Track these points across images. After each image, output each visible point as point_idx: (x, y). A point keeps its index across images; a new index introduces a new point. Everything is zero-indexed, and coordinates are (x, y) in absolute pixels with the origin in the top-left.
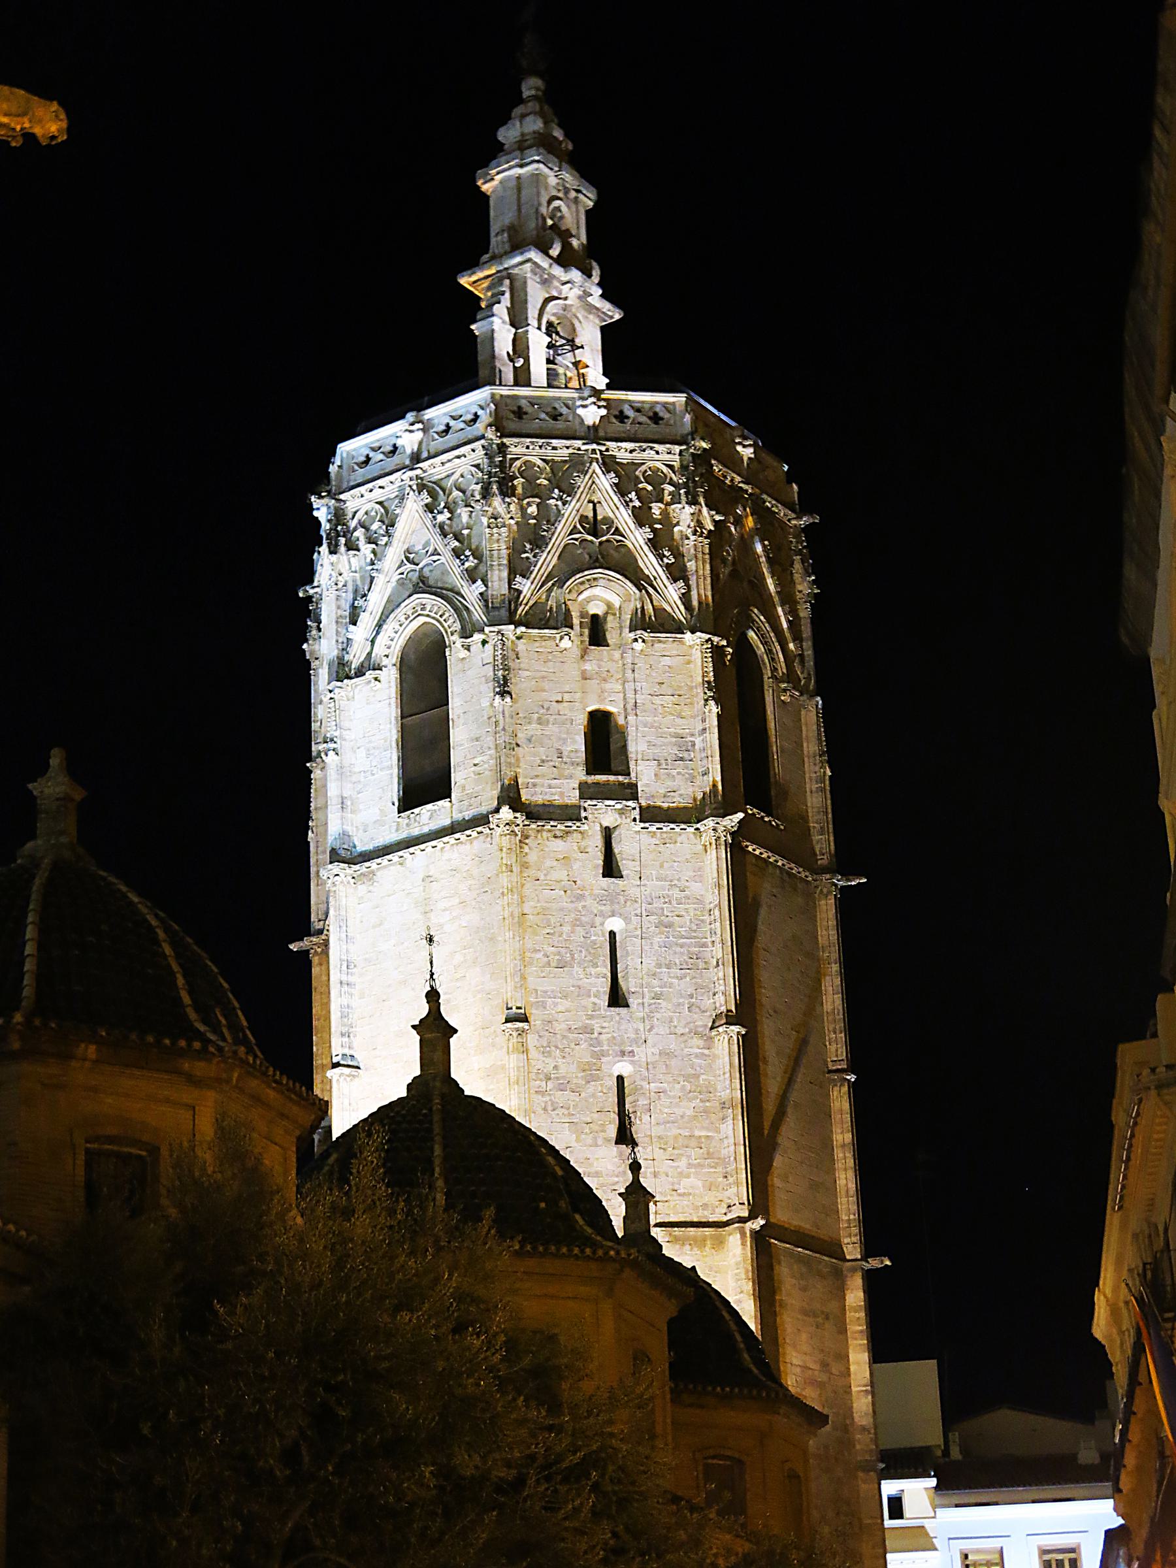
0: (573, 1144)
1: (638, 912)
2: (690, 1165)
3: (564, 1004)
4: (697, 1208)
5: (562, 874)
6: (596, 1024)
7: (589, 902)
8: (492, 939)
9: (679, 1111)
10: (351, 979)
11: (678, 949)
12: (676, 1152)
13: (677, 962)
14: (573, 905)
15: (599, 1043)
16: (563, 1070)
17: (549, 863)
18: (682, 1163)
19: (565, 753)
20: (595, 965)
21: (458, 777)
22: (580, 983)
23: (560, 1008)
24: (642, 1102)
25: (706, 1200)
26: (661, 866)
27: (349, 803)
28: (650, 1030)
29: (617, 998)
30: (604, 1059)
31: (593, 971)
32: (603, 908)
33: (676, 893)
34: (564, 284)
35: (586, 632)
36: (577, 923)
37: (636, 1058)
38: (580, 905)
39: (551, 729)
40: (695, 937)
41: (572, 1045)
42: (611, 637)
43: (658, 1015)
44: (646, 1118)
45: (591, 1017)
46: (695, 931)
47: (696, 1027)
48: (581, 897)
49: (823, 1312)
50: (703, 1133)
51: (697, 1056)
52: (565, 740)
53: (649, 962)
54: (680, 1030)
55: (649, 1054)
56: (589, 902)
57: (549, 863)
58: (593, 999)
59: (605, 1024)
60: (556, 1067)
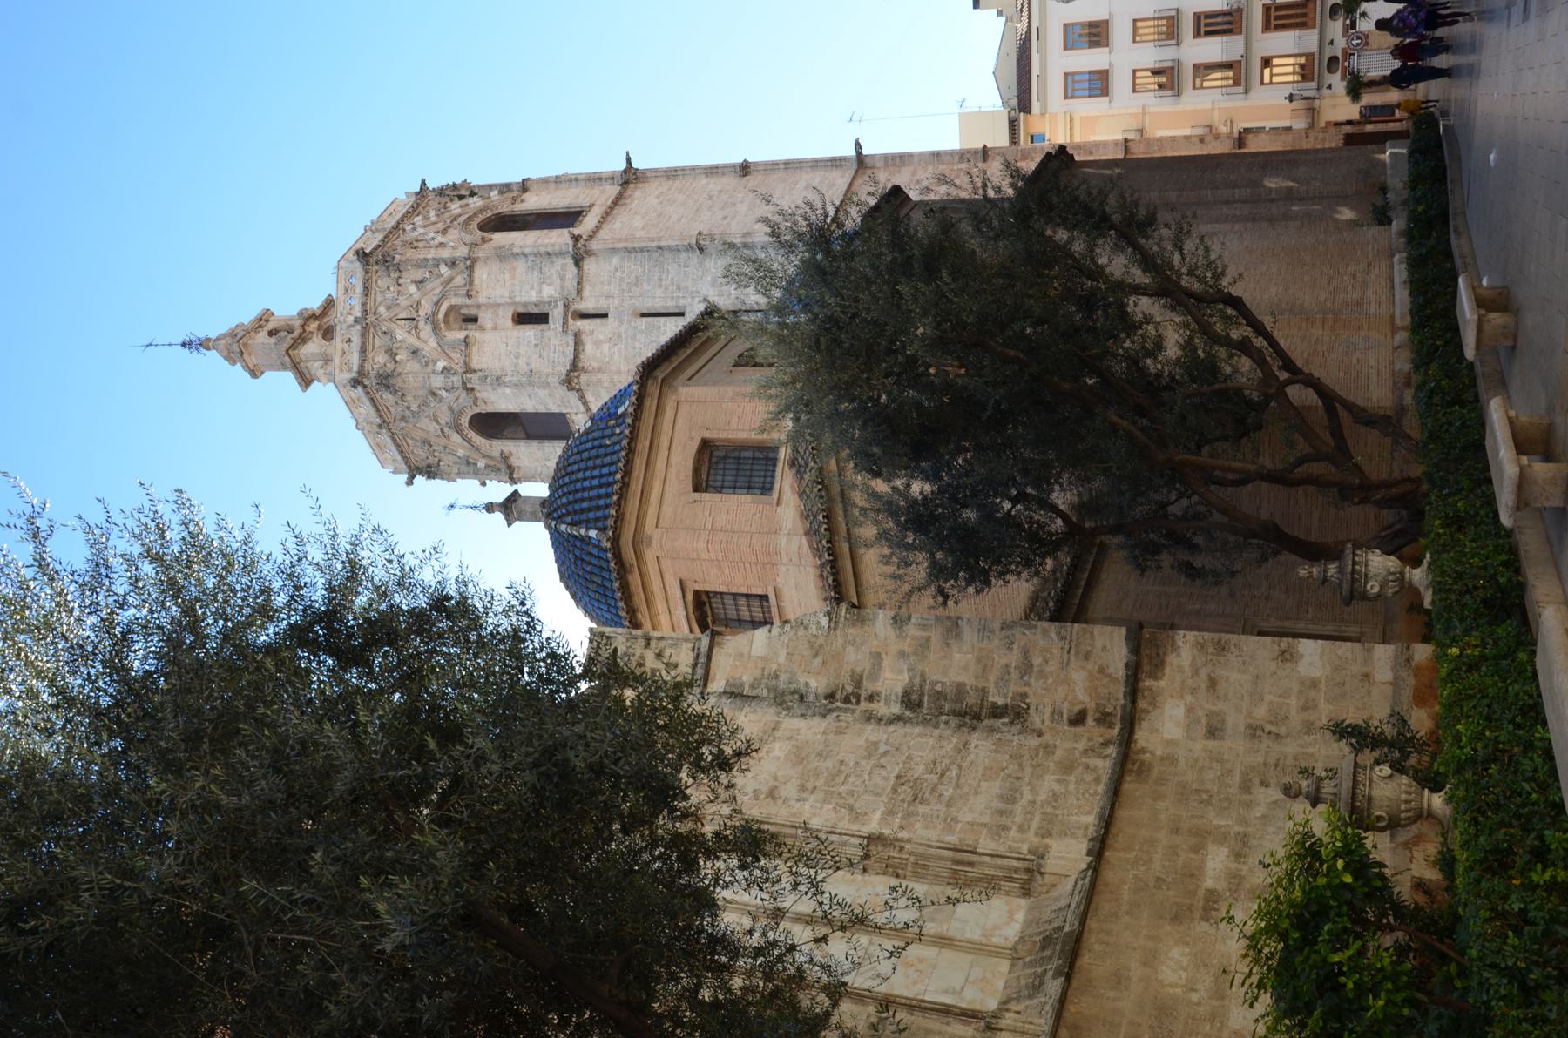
5: (606, 347)
36: (634, 338)
39: (522, 350)
42: (473, 312)
53: (659, 293)
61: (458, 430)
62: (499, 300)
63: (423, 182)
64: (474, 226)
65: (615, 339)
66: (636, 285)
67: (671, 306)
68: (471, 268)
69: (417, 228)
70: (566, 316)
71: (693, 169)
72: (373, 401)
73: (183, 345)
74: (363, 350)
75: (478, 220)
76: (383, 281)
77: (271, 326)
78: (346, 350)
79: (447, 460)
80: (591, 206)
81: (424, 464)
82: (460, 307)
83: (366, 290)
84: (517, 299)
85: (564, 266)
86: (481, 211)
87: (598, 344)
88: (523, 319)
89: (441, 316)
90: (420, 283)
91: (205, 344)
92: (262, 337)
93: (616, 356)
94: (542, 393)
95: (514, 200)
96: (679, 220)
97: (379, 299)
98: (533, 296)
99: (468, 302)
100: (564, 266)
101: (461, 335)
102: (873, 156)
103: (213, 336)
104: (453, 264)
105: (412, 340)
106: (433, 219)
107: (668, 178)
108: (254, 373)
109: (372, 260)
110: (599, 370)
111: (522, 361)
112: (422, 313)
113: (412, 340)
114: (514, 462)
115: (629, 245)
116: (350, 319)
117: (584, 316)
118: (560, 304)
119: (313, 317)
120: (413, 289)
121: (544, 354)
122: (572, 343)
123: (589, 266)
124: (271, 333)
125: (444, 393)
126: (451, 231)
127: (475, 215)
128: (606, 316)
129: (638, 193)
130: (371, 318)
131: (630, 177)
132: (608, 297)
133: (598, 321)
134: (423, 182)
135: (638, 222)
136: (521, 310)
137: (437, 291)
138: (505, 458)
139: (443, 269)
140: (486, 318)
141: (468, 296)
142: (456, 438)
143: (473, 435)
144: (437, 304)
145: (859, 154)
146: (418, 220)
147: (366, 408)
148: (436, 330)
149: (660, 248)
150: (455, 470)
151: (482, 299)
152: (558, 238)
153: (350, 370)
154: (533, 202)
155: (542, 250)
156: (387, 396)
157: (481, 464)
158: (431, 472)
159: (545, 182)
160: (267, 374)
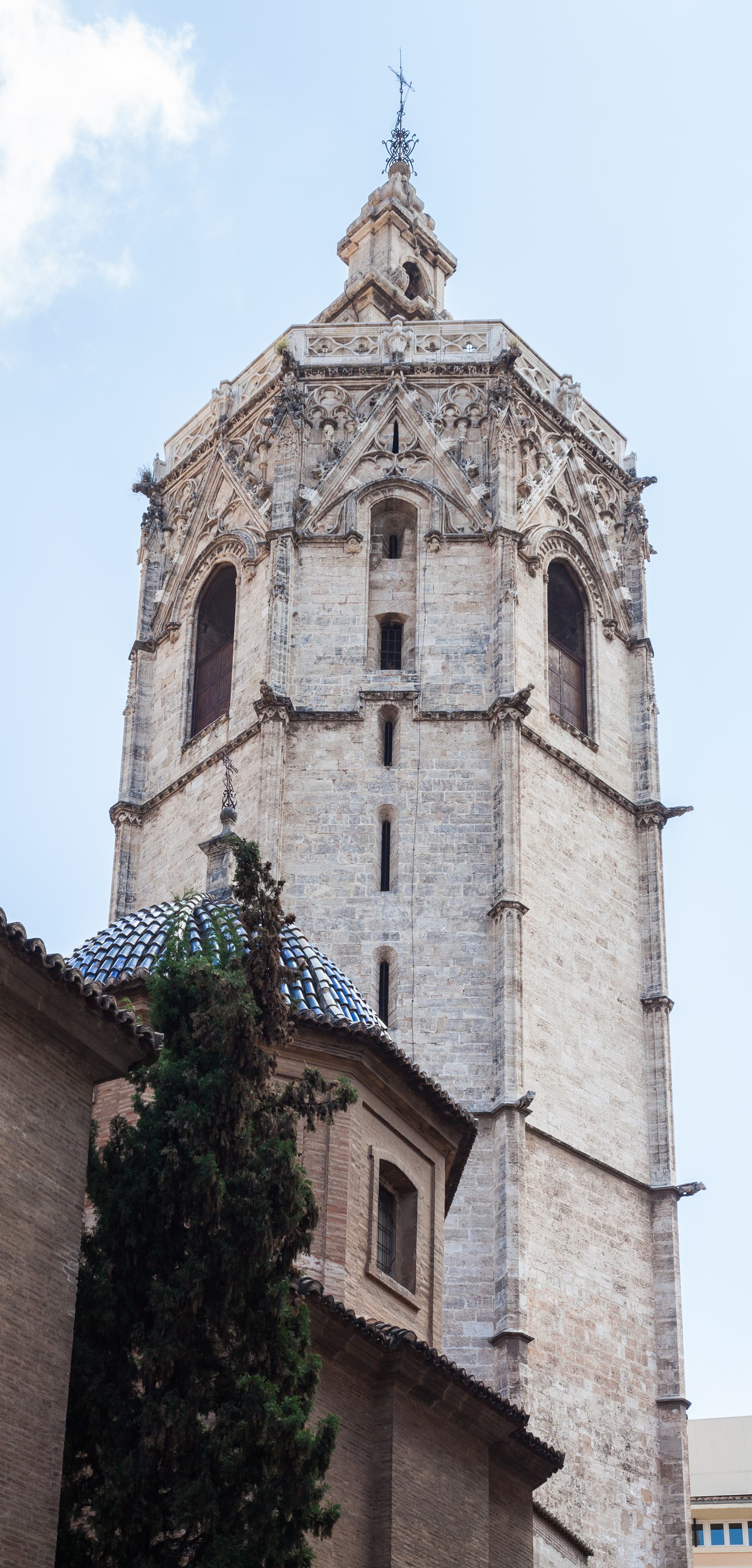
1: (415, 797)
2: (454, 1049)
3: (324, 889)
6: (358, 908)
7: (360, 789)
9: (446, 996)
11: (457, 834)
12: (439, 1035)
13: (455, 845)
14: (341, 793)
15: (360, 927)
19: (345, 650)
20: (361, 850)
22: (342, 868)
25: (471, 1085)
26: (444, 754)
27: (143, 752)
28: (418, 914)
29: (385, 885)
30: (364, 943)
31: (358, 855)
32: (375, 795)
33: (458, 779)
35: (380, 545)
36: (344, 809)
37: (401, 941)
38: (349, 793)
40: (477, 822)
41: (329, 929)
42: (406, 550)
43: (429, 898)
44: (407, 1002)
45: (352, 901)
46: (477, 816)
47: (473, 909)
49: (620, 1232)
51: (471, 939)
52: (345, 639)
53: (422, 848)
54: (453, 913)
55: (416, 935)
58: (357, 883)
59: (367, 908)
62: (420, 587)
65: (345, 780)
66: (438, 809)
67: (400, 867)
82: (414, 528)
84: (421, 616)
85: (476, 689)
86: (591, 568)
96: (556, 884)
100: (476, 689)
106: (580, 490)
115: (505, 793)
118: (410, 686)
122: (340, 708)
123: (473, 732)
126: (555, 515)
127: (585, 558)
128: (387, 758)
132: (418, 764)
135: (557, 818)
136: (407, 627)
140: (392, 570)
145: (677, 1193)
149: (500, 843)
151: (424, 559)
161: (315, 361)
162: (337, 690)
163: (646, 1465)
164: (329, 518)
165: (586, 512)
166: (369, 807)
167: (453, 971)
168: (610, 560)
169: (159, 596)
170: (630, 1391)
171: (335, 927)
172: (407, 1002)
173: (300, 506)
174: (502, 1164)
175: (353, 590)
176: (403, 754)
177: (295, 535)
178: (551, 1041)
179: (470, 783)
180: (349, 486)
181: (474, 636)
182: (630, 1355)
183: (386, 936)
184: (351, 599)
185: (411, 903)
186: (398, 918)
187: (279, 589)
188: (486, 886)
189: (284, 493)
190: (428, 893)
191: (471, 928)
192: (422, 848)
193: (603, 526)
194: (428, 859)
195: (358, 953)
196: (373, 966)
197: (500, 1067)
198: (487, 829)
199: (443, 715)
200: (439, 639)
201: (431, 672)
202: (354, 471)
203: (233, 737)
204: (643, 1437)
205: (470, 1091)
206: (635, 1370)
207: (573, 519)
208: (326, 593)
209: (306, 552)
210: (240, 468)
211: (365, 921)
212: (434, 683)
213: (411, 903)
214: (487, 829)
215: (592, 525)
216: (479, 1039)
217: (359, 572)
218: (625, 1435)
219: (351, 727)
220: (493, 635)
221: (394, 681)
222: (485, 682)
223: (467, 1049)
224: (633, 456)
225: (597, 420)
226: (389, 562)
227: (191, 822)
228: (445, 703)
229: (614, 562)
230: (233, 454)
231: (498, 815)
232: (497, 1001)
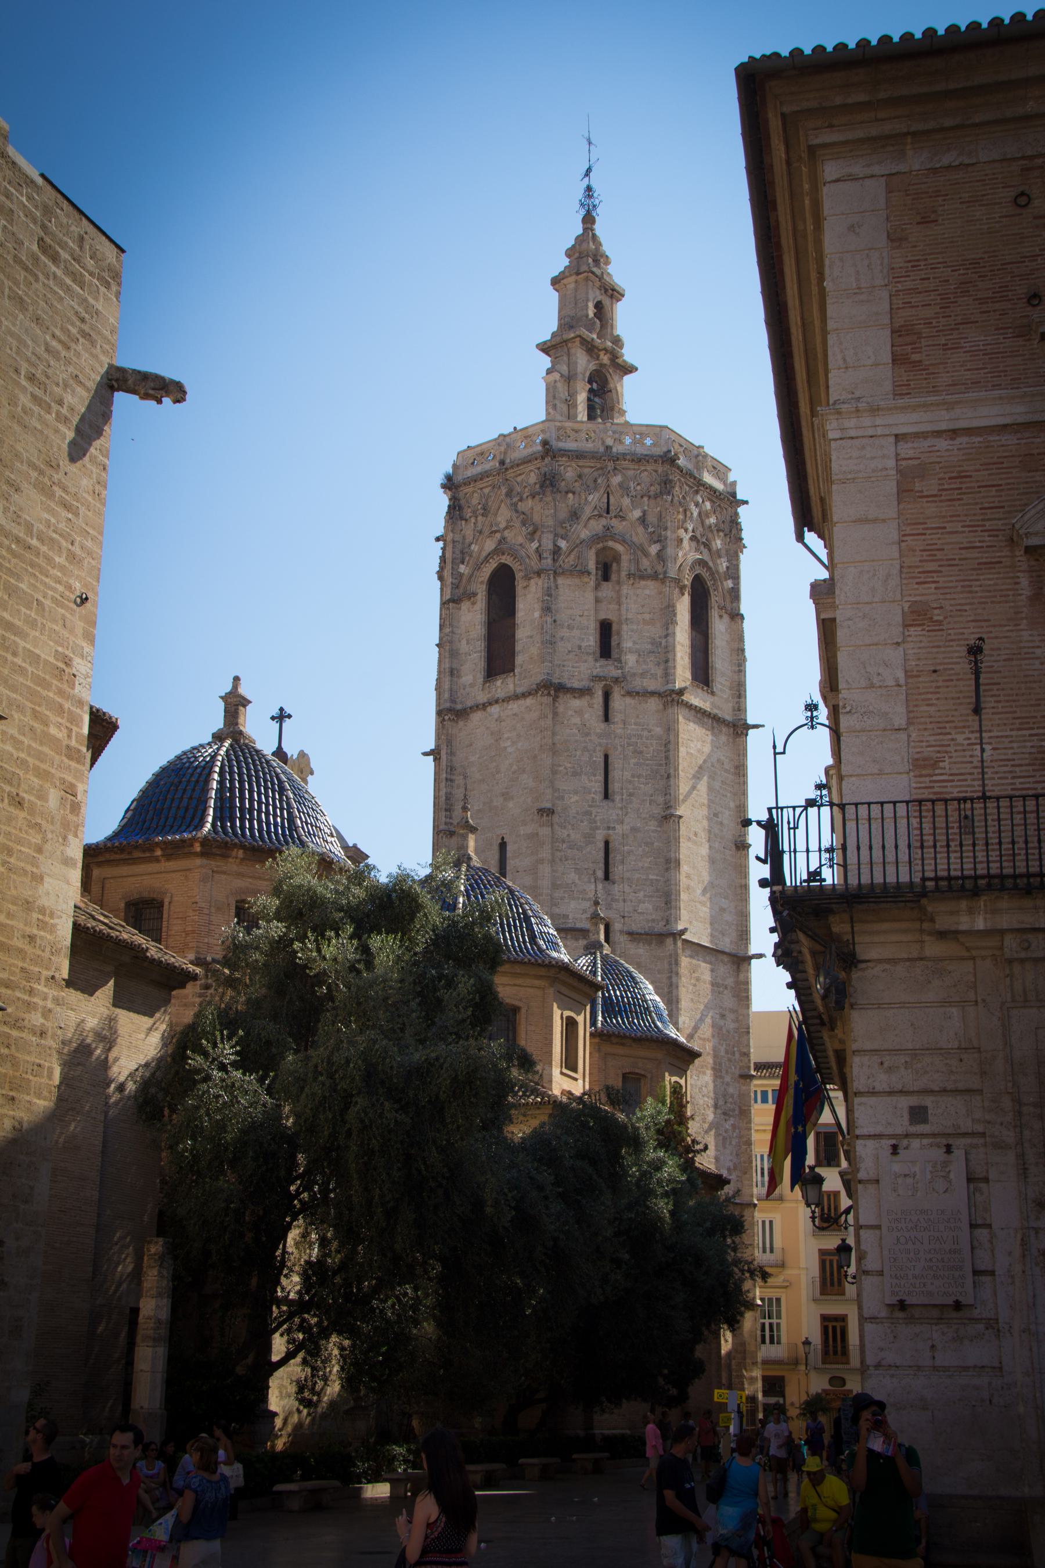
0: (577, 881)
2: (645, 896)
3: (575, 798)
4: (648, 921)
5: (577, 720)
6: (594, 810)
7: (593, 737)
8: (535, 757)
9: (640, 864)
10: (453, 777)
15: (595, 822)
16: (573, 836)
17: (570, 713)
18: (641, 894)
20: (595, 775)
21: (519, 660)
23: (572, 800)
24: (619, 857)
25: (654, 917)
26: (638, 717)
29: (606, 796)
33: (645, 733)
34: (600, 350)
35: (600, 572)
36: (585, 749)
39: (576, 633)
42: (614, 577)
44: (620, 867)
45: (590, 806)
48: (588, 734)
50: (655, 877)
51: (653, 831)
53: (627, 775)
54: (644, 816)
55: (625, 828)
56: (593, 737)
57: (570, 713)
60: (568, 835)
61: (497, 552)
63: (746, 502)
64: (698, 570)
66: (635, 752)
67: (615, 786)
68: (655, 577)
69: (699, 505)
70: (605, 678)
71: (744, 793)
72: (527, 461)
73: (589, 189)
74: (579, 455)
75: (705, 575)
76: (647, 475)
77: (606, 301)
78: (583, 432)
79: (468, 530)
80: (713, 693)
81: (462, 502)
83: (639, 460)
84: (625, 627)
85: (654, 676)
86: (712, 574)
87: (580, 712)
88: (606, 629)
89: (610, 544)
90: (643, 520)
91: (589, 220)
92: (595, 295)
93: (568, 731)
94: (534, 651)
95: (721, 608)
97: (630, 473)
98: (627, 644)
99: (623, 574)
100: (654, 676)
101: (592, 566)
102: (748, 971)
103: (599, 229)
104: (661, 556)
105: (588, 511)
107: (737, 767)
108: (555, 282)
109: (667, 467)
110: (555, 714)
111: (564, 632)
112: (615, 522)
113: (588, 511)
114: (465, 605)
116: (609, 442)
117: (607, 696)
118: (617, 673)
119: (615, 356)
120: (637, 514)
121: (571, 656)
123: (653, 704)
124: (599, 306)
125: (535, 545)
126: (694, 544)
127: (709, 569)
128: (607, 718)
129: (723, 738)
130: (610, 465)
131: (738, 728)
133: (601, 713)
134: (746, 502)
136: (615, 627)
137: (635, 539)
138: (471, 596)
139: (654, 549)
140: (607, 590)
141: (629, 576)
142: (490, 545)
143: (492, 565)
144: (623, 542)
146: (708, 505)
147: (522, 450)
148: (597, 538)
149: (669, 777)
150: (458, 537)
151: (625, 589)
152: (683, 674)
153: (558, 439)
154: (719, 626)
155: (670, 657)
156: (533, 478)
157: (462, 568)
158: (455, 512)
159: (739, 638)
160: (555, 295)
161: (561, 445)
162: (580, 672)
163: (734, 1110)
164: (572, 556)
165: (710, 535)
166: (598, 748)
167: (644, 850)
168: (723, 564)
169: (462, 568)
170: (727, 1072)
171: (582, 822)
172: (620, 867)
173: (556, 551)
174: (670, 964)
175: (586, 607)
176: (617, 717)
177: (555, 572)
178: (692, 884)
179: (652, 736)
180: (583, 536)
181: (653, 642)
182: (727, 1052)
183: (609, 828)
184: (586, 613)
185: (621, 809)
186: (615, 817)
187: (547, 610)
188: (661, 799)
189: (547, 543)
190: (631, 802)
191: (653, 825)
192: (627, 775)
193: (718, 543)
194: (630, 782)
195: (594, 837)
196: (601, 845)
197: (670, 908)
198: (661, 765)
199: (638, 693)
200: (635, 643)
201: (630, 664)
202: (585, 526)
203: (519, 690)
204: (732, 1096)
205: (653, 920)
206: (730, 1060)
207: (703, 543)
208: (572, 608)
209: (560, 581)
210: (515, 505)
211: (598, 818)
212: (632, 671)
213: (621, 809)
214: (661, 765)
215: (713, 544)
216: (658, 890)
217: (590, 596)
218: (724, 1096)
219: (587, 698)
220: (663, 641)
221: (610, 669)
222: (659, 672)
223: (651, 896)
224: (734, 483)
225: (715, 464)
226: (605, 584)
227: (492, 733)
228: (638, 684)
229: (724, 565)
230: (509, 494)
231: (667, 758)
232: (667, 869)
